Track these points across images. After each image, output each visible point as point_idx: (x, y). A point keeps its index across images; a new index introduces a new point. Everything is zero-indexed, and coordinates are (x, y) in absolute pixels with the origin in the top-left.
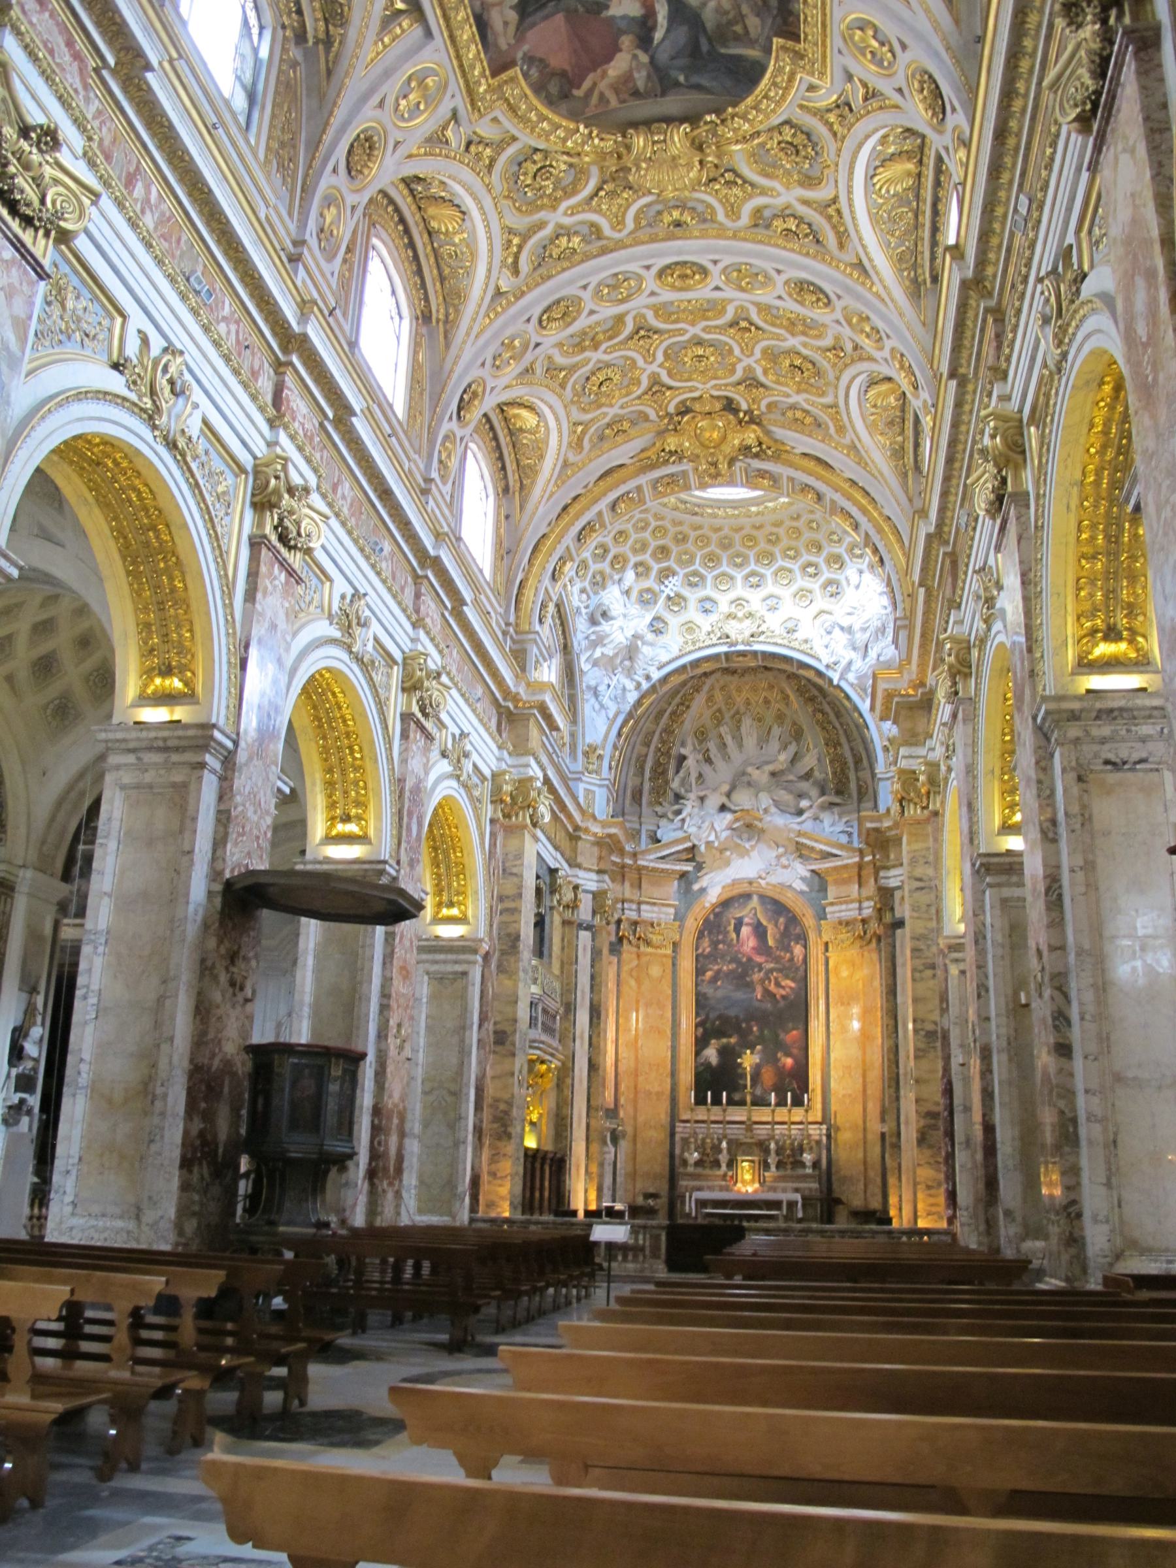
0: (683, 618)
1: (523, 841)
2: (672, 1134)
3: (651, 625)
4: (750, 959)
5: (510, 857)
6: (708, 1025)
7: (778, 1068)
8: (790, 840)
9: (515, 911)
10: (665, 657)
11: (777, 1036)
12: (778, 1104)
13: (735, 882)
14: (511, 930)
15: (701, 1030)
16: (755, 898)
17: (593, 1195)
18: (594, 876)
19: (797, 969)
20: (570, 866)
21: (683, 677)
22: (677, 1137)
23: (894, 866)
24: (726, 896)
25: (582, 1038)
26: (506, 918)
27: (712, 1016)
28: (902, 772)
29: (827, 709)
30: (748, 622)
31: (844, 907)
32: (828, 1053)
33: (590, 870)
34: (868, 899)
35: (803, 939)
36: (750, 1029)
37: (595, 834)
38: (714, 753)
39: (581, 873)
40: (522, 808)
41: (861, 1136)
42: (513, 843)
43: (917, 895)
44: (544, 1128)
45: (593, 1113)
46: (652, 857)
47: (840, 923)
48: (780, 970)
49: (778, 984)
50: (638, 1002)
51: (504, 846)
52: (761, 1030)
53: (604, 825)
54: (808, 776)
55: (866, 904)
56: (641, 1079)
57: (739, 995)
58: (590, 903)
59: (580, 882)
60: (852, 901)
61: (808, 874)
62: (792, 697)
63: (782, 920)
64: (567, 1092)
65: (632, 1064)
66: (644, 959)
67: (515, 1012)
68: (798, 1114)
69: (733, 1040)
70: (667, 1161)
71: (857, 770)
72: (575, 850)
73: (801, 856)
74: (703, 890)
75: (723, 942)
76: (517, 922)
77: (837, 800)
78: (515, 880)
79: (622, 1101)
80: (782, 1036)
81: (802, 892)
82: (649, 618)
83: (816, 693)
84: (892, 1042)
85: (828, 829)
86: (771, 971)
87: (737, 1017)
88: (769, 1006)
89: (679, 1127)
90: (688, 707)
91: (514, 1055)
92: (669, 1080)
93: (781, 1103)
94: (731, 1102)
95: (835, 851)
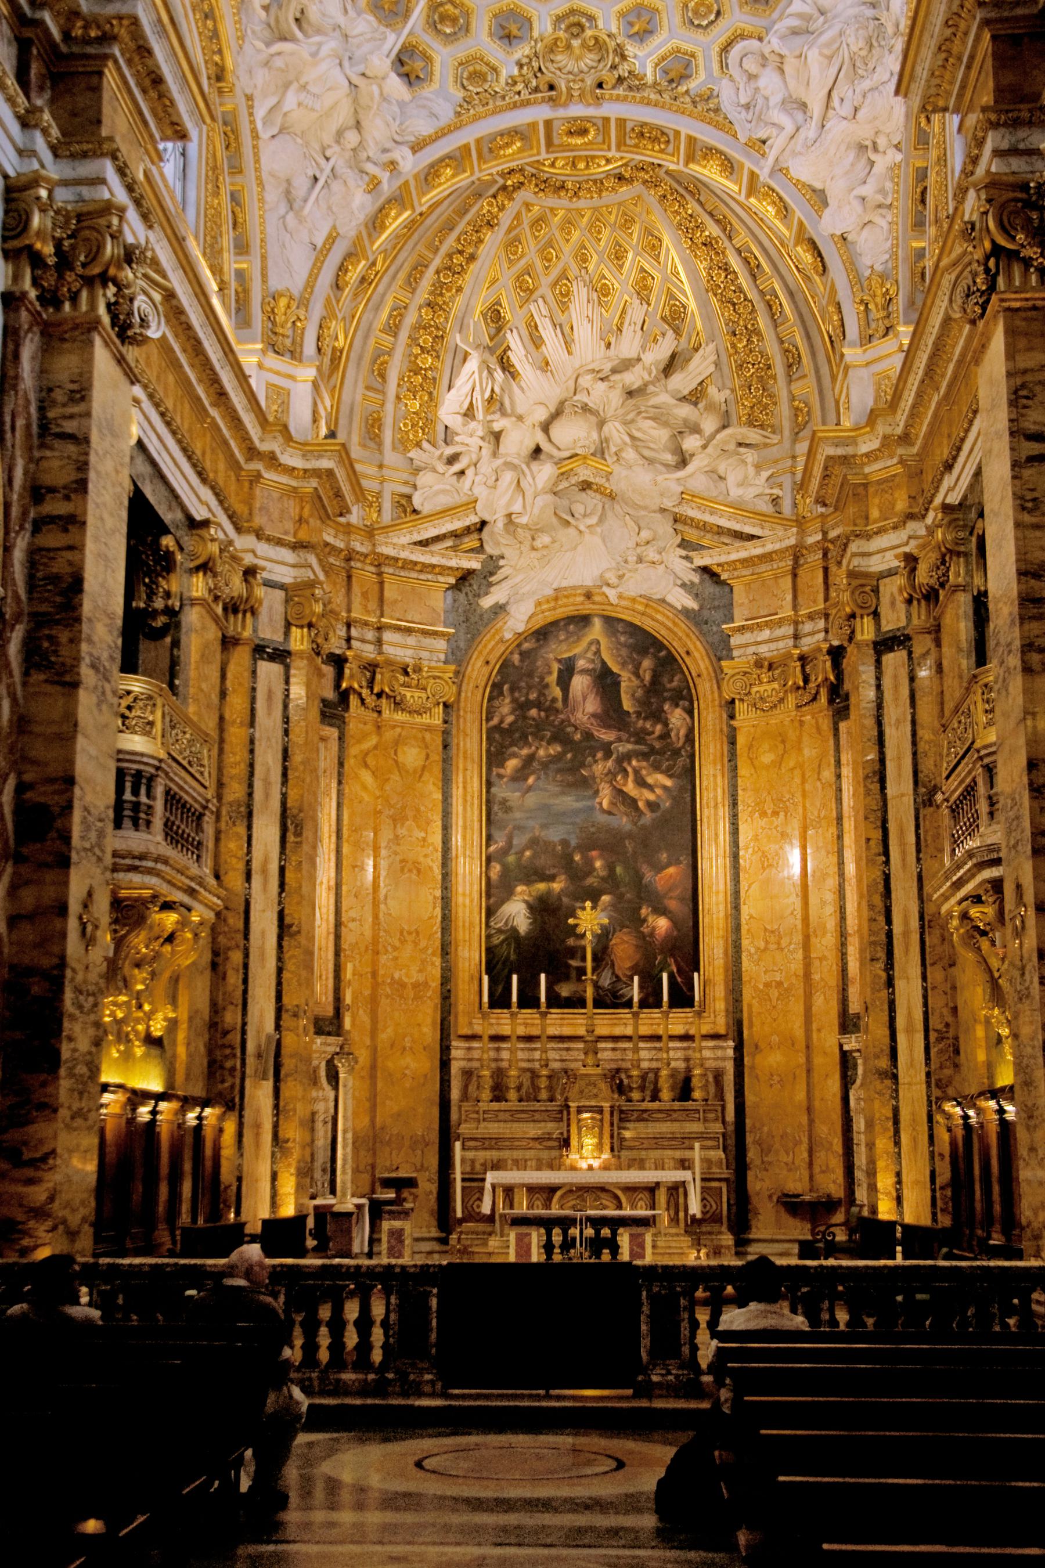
0: (463, 49)
1: (88, 361)
2: (445, 1064)
3: (400, 61)
4: (588, 736)
5: (59, 396)
6: (511, 859)
7: (642, 936)
8: (663, 510)
9: (74, 522)
10: (424, 127)
11: (638, 877)
12: (644, 1004)
13: (559, 594)
14: (60, 566)
15: (496, 868)
16: (597, 623)
17: (288, 1185)
18: (287, 555)
19: (677, 753)
20: (238, 529)
21: (464, 179)
22: (455, 1067)
23: (879, 532)
24: (539, 622)
25: (264, 871)
26: (52, 539)
27: (519, 841)
28: (993, 184)
29: (735, 262)
30: (590, 59)
31: (766, 634)
32: (737, 907)
33: (280, 542)
34: (811, 617)
35: (685, 697)
36: (589, 862)
37: (291, 471)
38: (518, 355)
39: (263, 548)
40: (89, 282)
41: (802, 1060)
42: (66, 365)
43: (1027, 473)
44: (181, 1051)
45: (287, 1020)
46: (405, 539)
47: (758, 664)
48: (644, 756)
49: (641, 783)
50: (378, 813)
51: (42, 372)
52: (611, 868)
53: (306, 449)
54: (695, 397)
55: (808, 627)
56: (383, 959)
57: (569, 802)
58: (279, 608)
59: (261, 563)
60: (780, 623)
61: (696, 578)
62: (667, 240)
63: (647, 663)
64: (234, 979)
65: (368, 933)
66: (389, 735)
67: (71, 762)
68: (679, 1022)
69: (557, 886)
70: (436, 1112)
71: (790, 380)
72: (249, 501)
73: (684, 544)
74: (500, 609)
75: (538, 705)
76: (77, 548)
77: (753, 435)
78: (71, 449)
79: (348, 998)
80: (648, 875)
81: (686, 612)
82: (393, 41)
83: (713, 230)
84: (877, 874)
85: (735, 492)
86: (627, 757)
87: (565, 843)
88: (623, 822)
89: (458, 1051)
90: (472, 258)
91: (64, 863)
92: (438, 961)
93: (652, 1000)
94: (555, 1001)
95: (748, 530)
